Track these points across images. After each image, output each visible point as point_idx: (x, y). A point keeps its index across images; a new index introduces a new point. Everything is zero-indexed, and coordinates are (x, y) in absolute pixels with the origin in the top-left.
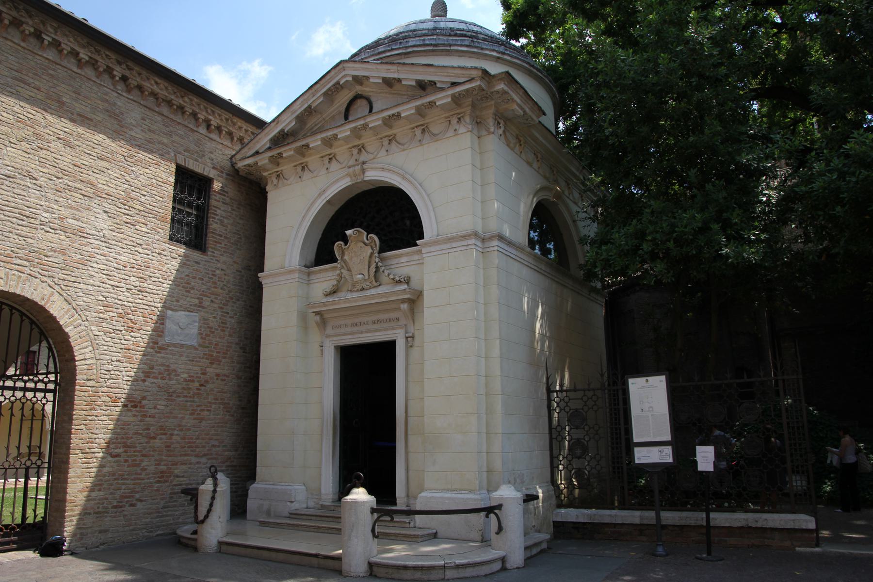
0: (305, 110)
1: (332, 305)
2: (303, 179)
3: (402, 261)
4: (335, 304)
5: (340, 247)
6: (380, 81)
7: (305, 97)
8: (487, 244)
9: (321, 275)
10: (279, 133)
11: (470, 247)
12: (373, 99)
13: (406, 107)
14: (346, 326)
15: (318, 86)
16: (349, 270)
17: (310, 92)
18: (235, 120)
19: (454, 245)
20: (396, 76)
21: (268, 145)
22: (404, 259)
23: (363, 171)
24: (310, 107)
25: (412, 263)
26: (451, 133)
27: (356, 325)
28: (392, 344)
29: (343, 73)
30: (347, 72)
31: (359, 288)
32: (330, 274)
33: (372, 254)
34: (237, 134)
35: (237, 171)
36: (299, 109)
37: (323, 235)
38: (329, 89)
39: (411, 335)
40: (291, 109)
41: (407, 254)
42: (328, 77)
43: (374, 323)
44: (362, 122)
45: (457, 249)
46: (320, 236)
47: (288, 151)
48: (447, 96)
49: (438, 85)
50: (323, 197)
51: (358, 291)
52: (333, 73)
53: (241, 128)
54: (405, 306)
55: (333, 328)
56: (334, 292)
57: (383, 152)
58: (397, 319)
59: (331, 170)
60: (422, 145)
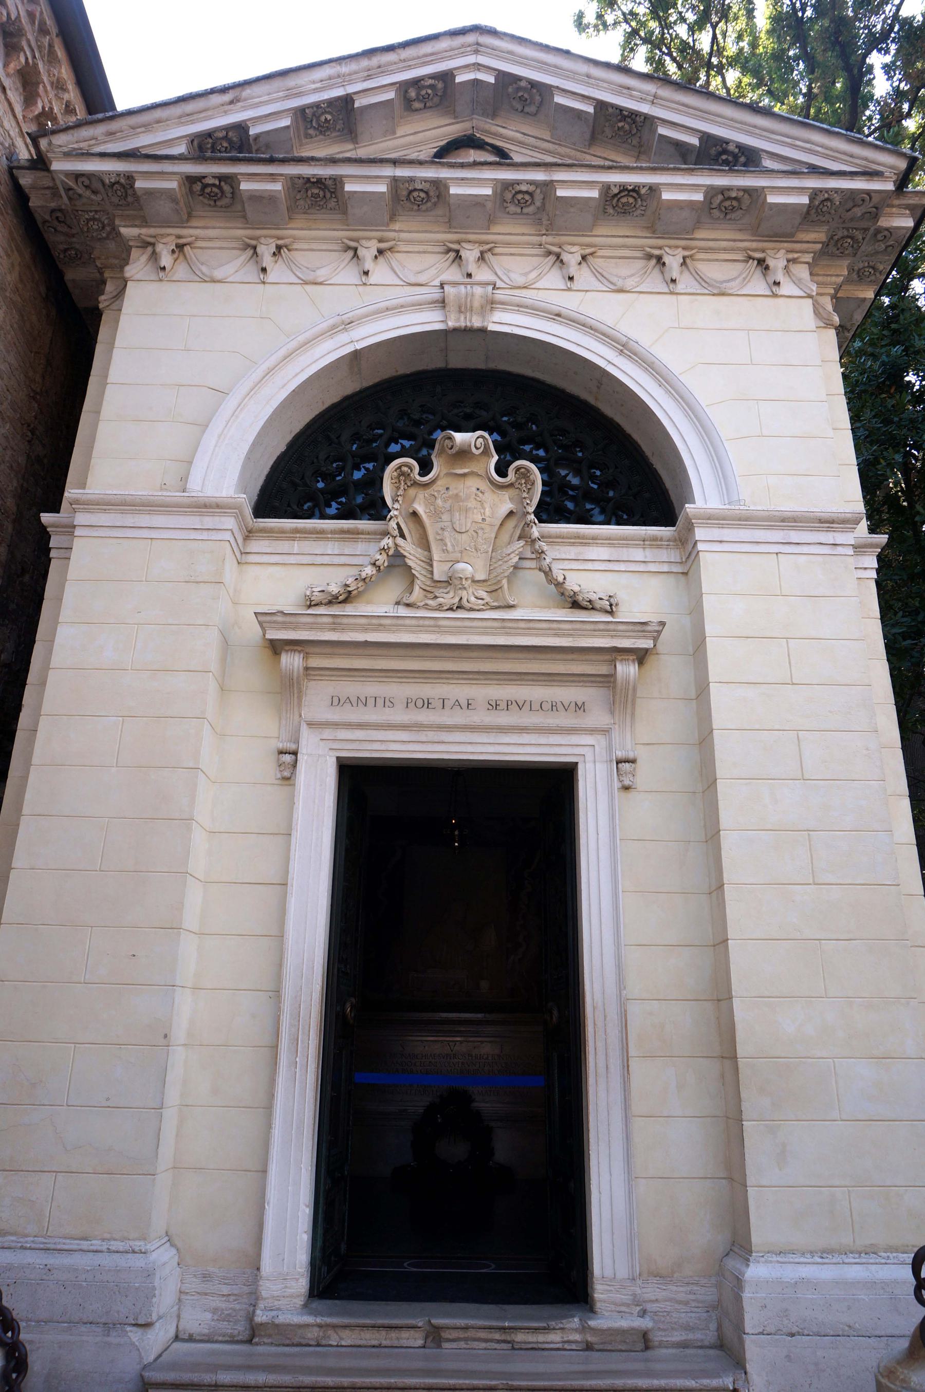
0: (331, 102)
1: (365, 629)
2: (271, 277)
4: (380, 628)
5: (402, 473)
6: (590, 109)
7: (344, 69)
9: (296, 546)
10: (228, 128)
11: (840, 550)
14: (388, 702)
15: (391, 57)
16: (425, 544)
17: (365, 63)
18: (60, 52)
19: (794, 536)
20: (645, 108)
21: (181, 149)
24: (348, 100)
25: (622, 567)
26: (758, 285)
29: (472, 59)
30: (482, 59)
31: (448, 598)
32: (331, 547)
33: (511, 513)
34: (47, 99)
35: (20, 196)
36: (314, 94)
37: (291, 445)
38: (416, 83)
39: (631, 755)
40: (291, 82)
41: (609, 541)
42: (427, 48)
43: (494, 706)
44: (539, 176)
45: (805, 549)
46: (282, 448)
48: (801, 190)
49: (768, 163)
50: (343, 338)
51: (439, 608)
52: (444, 44)
53: (60, 94)
54: (627, 670)
55: (336, 702)
57: (554, 279)
58: (580, 707)
59: (373, 279)
60: (672, 293)
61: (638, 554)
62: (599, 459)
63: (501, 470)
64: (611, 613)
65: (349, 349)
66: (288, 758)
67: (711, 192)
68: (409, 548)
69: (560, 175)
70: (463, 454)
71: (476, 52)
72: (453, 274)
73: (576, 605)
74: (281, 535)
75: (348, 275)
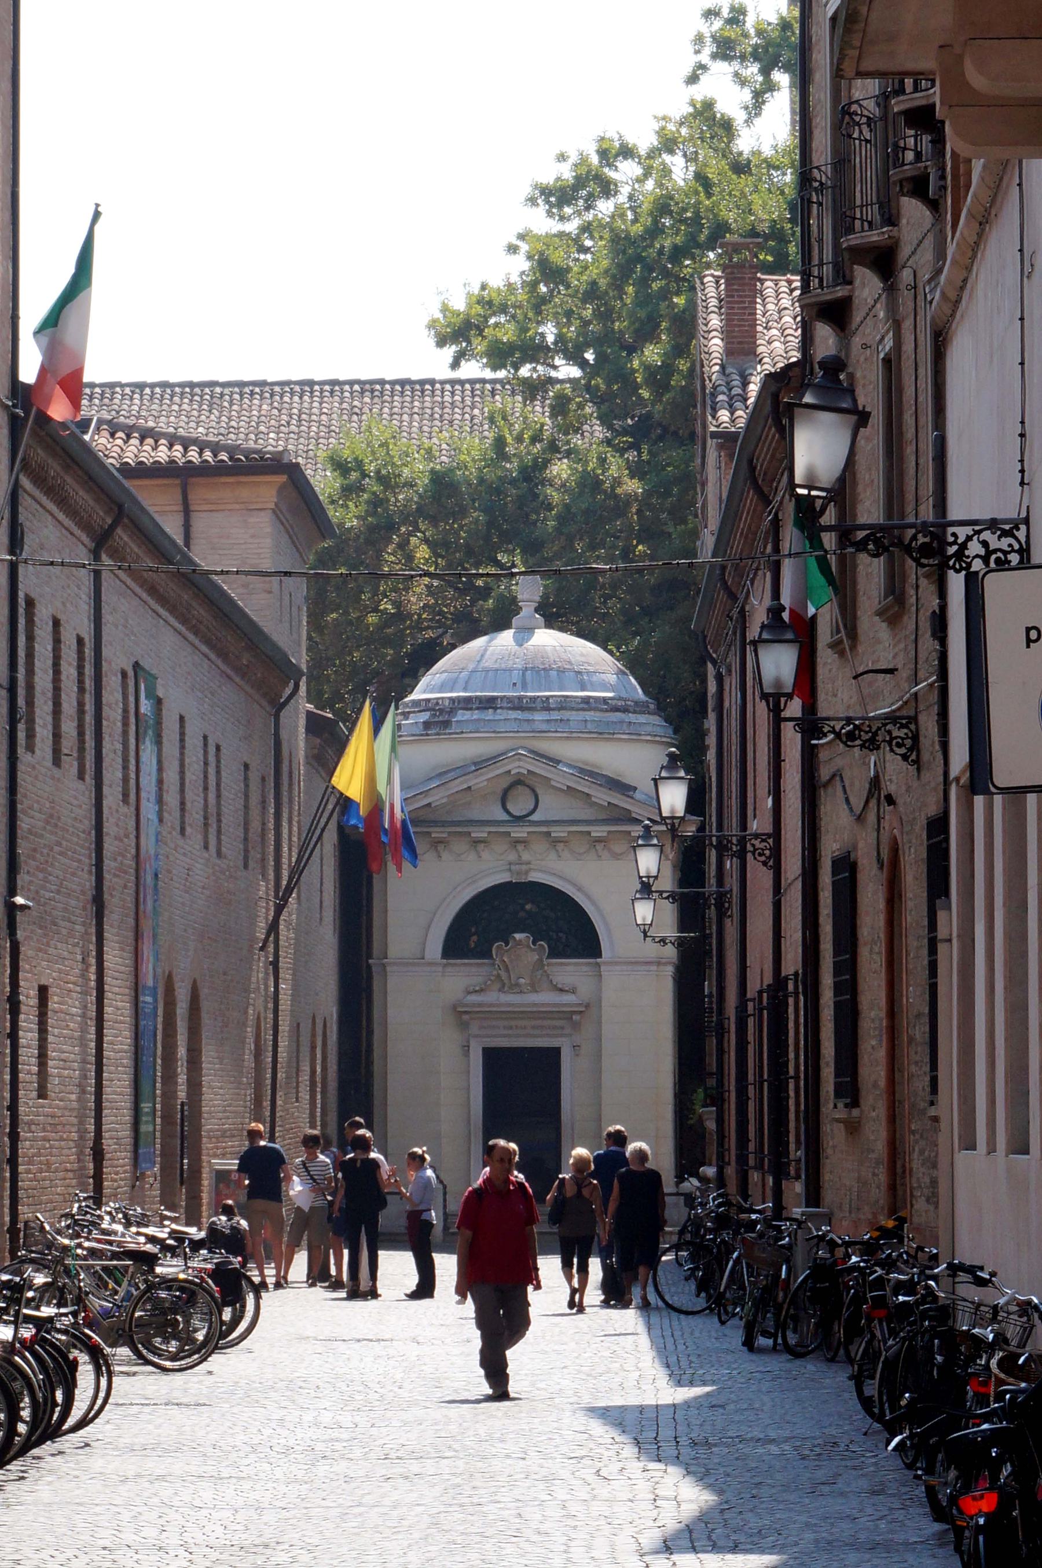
3: (571, 972)
8: (662, 968)
12: (539, 791)
13: (597, 828)
16: (507, 970)
20: (586, 790)
22: (568, 968)
23: (527, 873)
27: (511, 1028)
28: (557, 1051)
32: (474, 969)
41: (576, 964)
43: (533, 1027)
44: (544, 829)
47: (437, 833)
55: (481, 1028)
56: (482, 990)
57: (553, 855)
58: (562, 1028)
61: (585, 968)
62: (571, 931)
63: (534, 943)
64: (573, 991)
65: (475, 892)
66: (466, 1049)
67: (609, 832)
68: (502, 973)
69: (552, 829)
70: (519, 943)
71: (519, 760)
72: (512, 857)
73: (561, 990)
74: (455, 965)
75: (472, 856)
